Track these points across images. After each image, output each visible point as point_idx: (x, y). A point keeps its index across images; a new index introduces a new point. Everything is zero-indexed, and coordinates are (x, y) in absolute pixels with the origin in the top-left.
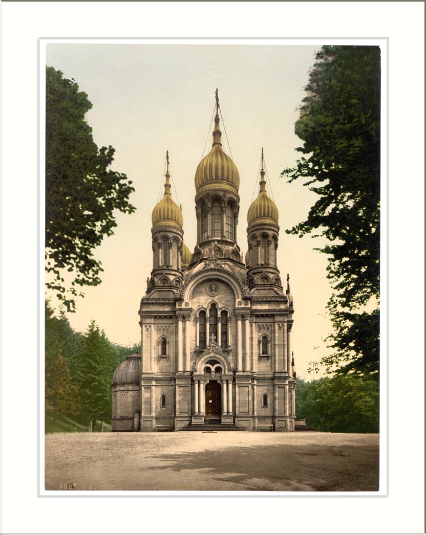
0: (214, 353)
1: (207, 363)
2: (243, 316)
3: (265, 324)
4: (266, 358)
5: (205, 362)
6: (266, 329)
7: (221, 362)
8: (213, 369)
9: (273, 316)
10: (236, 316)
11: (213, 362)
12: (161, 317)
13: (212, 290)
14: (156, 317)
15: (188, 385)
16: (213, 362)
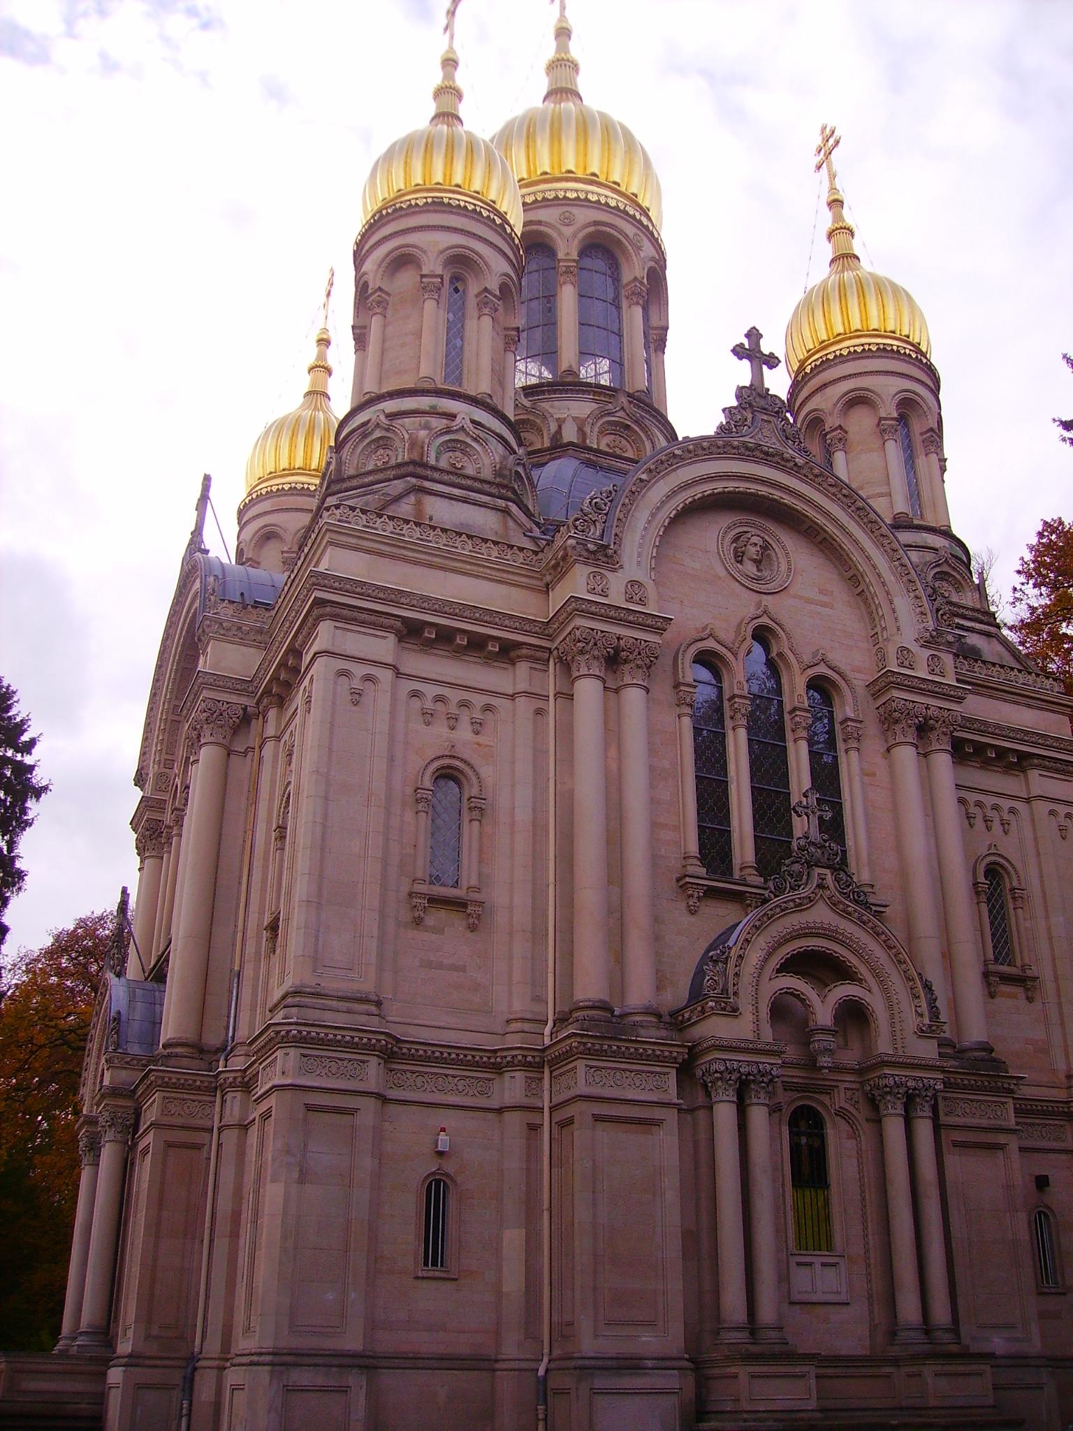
0: (833, 905)
1: (787, 967)
2: (923, 730)
3: (989, 801)
4: (1019, 991)
5: (775, 961)
6: (996, 826)
7: (863, 970)
8: (823, 1012)
9: (1019, 763)
10: (889, 720)
11: (819, 966)
12: (445, 637)
13: (739, 557)
14: (410, 633)
15: (658, 1113)
16: (819, 966)
